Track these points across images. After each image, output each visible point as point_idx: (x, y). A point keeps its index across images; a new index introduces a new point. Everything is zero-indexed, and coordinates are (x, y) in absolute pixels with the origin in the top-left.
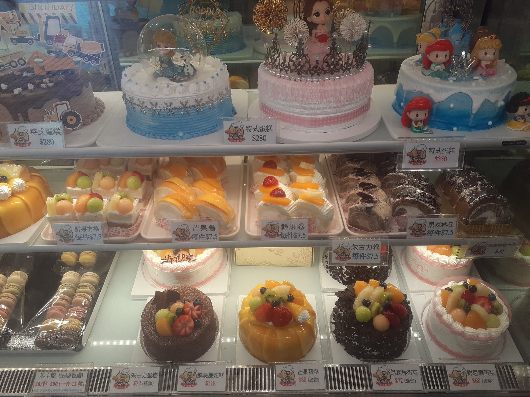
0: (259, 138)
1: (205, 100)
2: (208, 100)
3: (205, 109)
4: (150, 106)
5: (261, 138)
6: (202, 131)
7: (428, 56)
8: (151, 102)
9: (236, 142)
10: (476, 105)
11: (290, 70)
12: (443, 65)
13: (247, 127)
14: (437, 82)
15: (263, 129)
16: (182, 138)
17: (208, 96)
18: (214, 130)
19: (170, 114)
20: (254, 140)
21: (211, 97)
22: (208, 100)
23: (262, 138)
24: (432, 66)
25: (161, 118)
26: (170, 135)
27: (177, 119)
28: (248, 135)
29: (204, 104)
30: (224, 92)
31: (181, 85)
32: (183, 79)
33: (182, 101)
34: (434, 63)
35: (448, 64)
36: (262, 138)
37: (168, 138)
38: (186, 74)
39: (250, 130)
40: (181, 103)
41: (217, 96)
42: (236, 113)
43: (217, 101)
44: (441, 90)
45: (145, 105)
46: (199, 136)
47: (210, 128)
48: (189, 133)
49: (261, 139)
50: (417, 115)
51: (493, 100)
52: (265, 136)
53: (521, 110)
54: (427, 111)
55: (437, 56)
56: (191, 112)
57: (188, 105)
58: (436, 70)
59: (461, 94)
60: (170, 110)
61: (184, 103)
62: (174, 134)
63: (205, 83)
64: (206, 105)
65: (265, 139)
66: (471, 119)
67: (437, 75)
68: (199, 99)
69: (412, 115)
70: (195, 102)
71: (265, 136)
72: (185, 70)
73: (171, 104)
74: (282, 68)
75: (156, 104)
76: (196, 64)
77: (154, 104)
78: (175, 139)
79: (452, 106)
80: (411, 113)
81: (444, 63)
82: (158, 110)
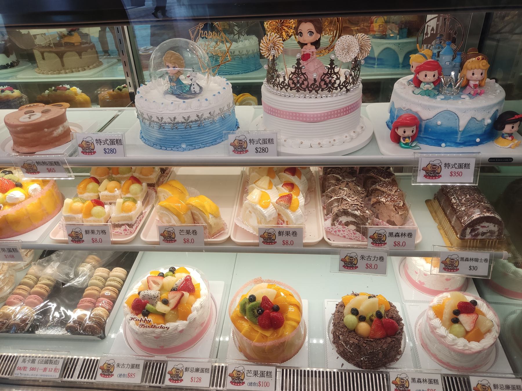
0: (262, 150)
1: (207, 115)
2: (209, 116)
3: (205, 123)
4: (157, 120)
5: (263, 150)
6: (203, 144)
7: (417, 75)
8: (158, 116)
9: (240, 153)
10: (463, 123)
11: (289, 88)
12: (432, 84)
13: (250, 140)
14: (426, 100)
15: (265, 141)
16: (184, 150)
17: (209, 112)
18: (215, 142)
19: (174, 128)
20: (257, 151)
21: (212, 113)
22: (209, 116)
23: (265, 150)
24: (422, 85)
25: (166, 131)
26: (174, 146)
27: (181, 132)
28: (251, 147)
29: (205, 119)
30: (226, 108)
31: (184, 102)
32: (189, 96)
33: (184, 116)
34: (424, 82)
35: (437, 83)
36: (264, 150)
37: (172, 149)
38: (193, 92)
39: (253, 143)
40: (184, 118)
41: (217, 111)
42: (238, 128)
43: (218, 117)
44: (429, 108)
45: (153, 119)
46: (200, 148)
47: (212, 141)
48: (191, 145)
49: (263, 151)
50: (405, 132)
51: (479, 118)
52: (267, 148)
53: (508, 128)
54: (414, 128)
55: (426, 76)
56: (192, 126)
57: (190, 120)
58: (426, 89)
59: (448, 111)
60: (174, 124)
61: (186, 118)
62: (178, 146)
63: (207, 100)
64: (207, 120)
65: (267, 151)
66: (459, 136)
67: (427, 93)
68: (200, 115)
69: (400, 132)
70: (197, 118)
71: (267, 148)
72: (192, 88)
73: (175, 118)
74: (282, 87)
75: (162, 118)
76: (202, 83)
77: (160, 118)
78: (178, 151)
79: (439, 123)
80: (399, 130)
81: (433, 82)
82: (164, 123)
